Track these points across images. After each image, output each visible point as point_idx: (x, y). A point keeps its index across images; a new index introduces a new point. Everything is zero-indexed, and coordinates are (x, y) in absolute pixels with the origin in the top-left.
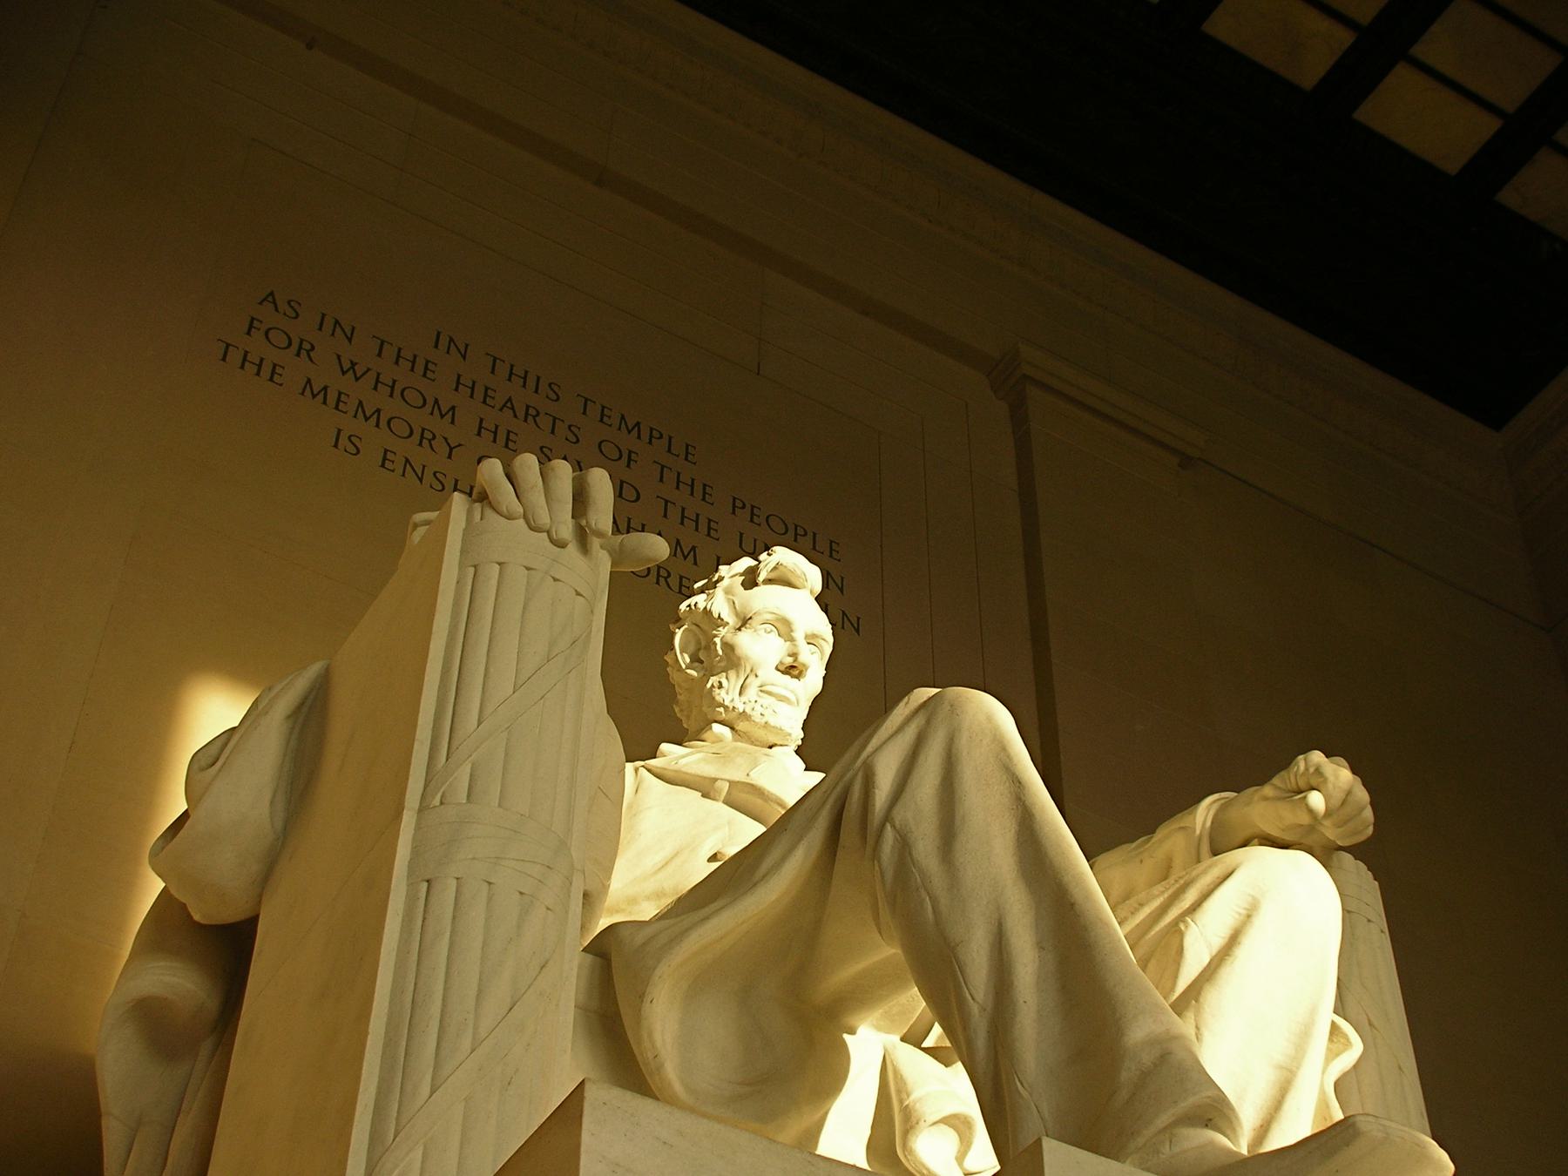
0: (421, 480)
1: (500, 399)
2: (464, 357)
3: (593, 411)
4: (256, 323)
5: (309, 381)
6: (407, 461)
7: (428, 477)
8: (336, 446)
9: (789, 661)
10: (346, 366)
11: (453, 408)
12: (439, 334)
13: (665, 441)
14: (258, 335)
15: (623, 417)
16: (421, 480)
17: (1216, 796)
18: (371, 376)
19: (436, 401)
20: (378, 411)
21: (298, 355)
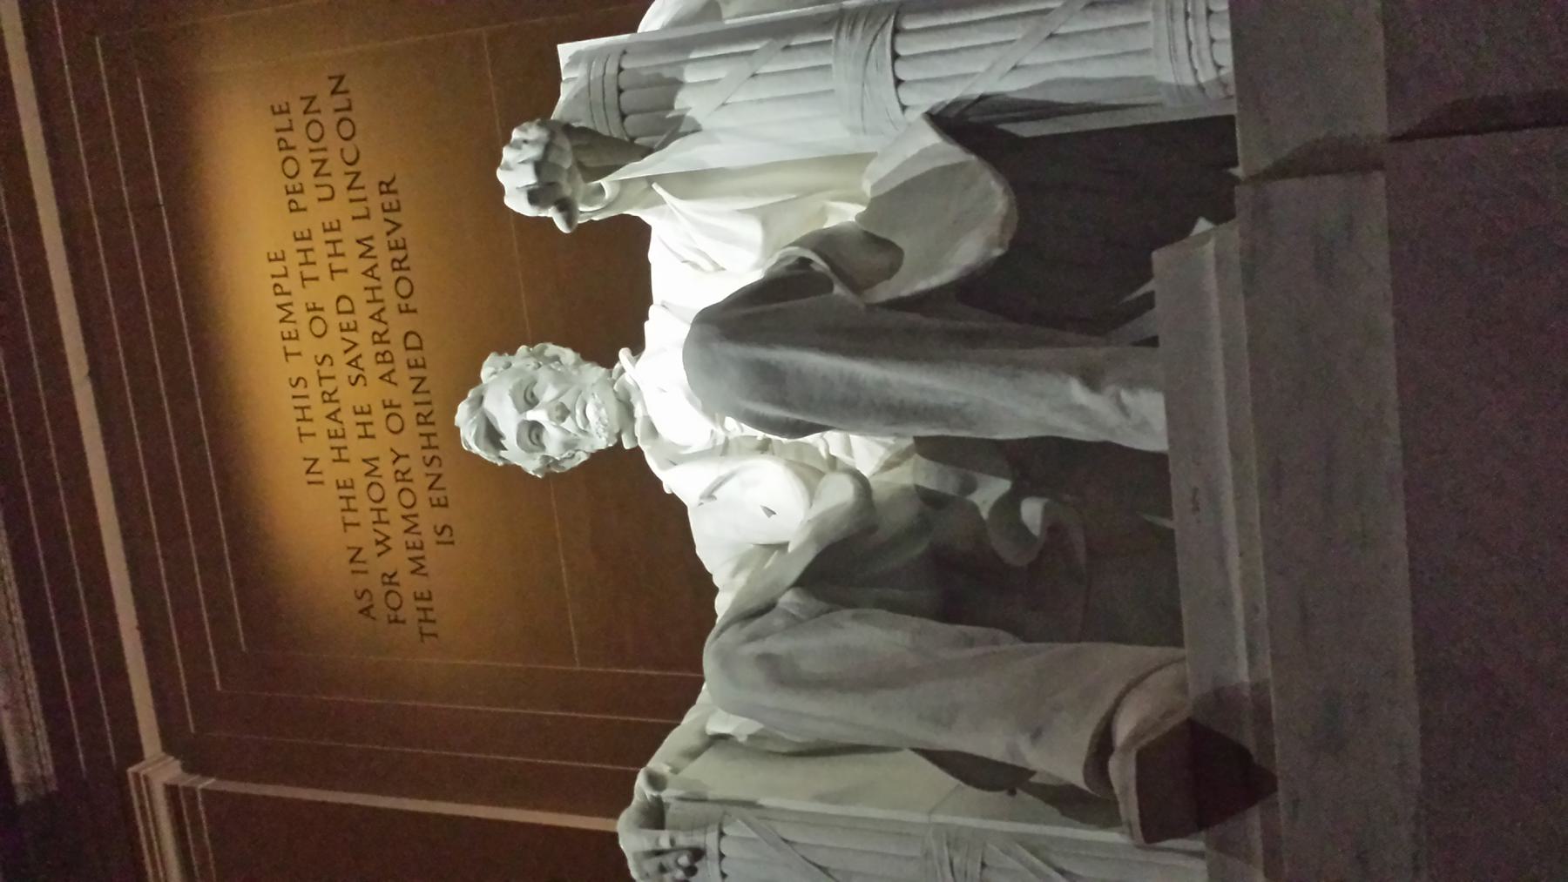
1: (334, 426)
3: (292, 346)
5: (413, 572)
6: (431, 488)
7: (434, 469)
10: (381, 548)
13: (276, 280)
14: (401, 615)
15: (282, 321)
16: (439, 476)
19: (367, 474)
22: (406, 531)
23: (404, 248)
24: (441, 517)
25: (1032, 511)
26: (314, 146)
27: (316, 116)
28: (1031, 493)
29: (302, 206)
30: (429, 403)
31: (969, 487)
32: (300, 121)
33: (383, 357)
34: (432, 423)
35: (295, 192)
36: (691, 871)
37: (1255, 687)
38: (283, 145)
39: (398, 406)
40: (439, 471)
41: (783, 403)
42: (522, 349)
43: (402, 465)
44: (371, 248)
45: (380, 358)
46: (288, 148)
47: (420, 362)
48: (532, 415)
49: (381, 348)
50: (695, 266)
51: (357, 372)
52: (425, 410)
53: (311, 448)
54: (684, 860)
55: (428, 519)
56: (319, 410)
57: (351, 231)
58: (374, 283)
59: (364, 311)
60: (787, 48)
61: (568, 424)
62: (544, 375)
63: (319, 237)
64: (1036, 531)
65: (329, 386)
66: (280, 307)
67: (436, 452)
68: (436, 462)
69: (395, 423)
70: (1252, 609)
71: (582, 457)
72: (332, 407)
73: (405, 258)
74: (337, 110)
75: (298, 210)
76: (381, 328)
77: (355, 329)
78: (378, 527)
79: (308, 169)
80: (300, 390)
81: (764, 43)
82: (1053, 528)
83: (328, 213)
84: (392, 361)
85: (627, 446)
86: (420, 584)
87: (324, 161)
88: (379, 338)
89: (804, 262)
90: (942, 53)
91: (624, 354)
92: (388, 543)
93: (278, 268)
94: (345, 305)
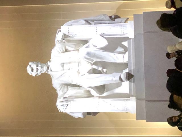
9: (40, 68)
25: (105, 70)
28: (104, 69)
31: (98, 68)
36: (67, 107)
37: (133, 70)
41: (89, 57)
48: (38, 68)
50: (59, 52)
54: (66, 106)
61: (42, 69)
64: (105, 71)
70: (133, 64)
71: (40, 74)
82: (106, 72)
89: (89, 45)
91: (48, 62)
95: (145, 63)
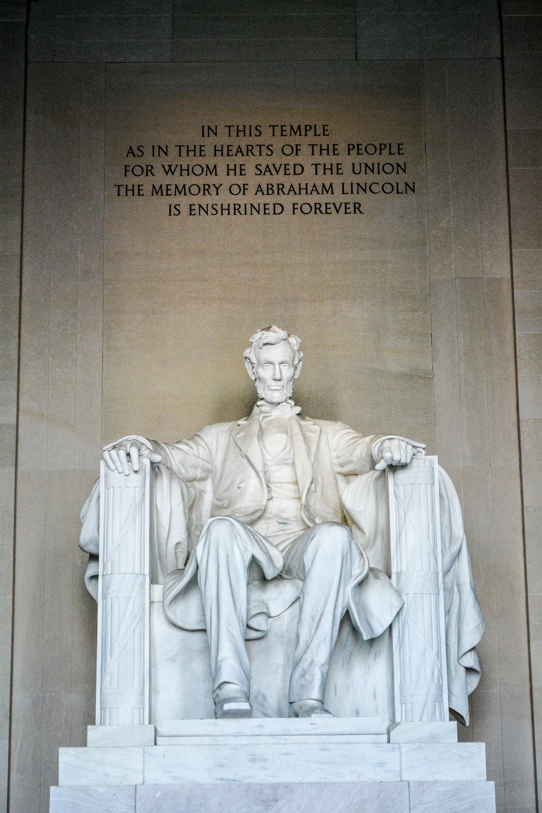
0: (207, 213)
2: (216, 134)
4: (128, 169)
5: (154, 186)
6: (200, 206)
7: (210, 210)
8: (170, 215)
10: (167, 168)
11: (215, 166)
12: (203, 127)
14: (129, 173)
16: (207, 213)
17: (378, 441)
18: (178, 169)
19: (208, 166)
20: (184, 186)
21: (147, 175)
22: (176, 186)
23: (327, 213)
24: (185, 210)
26: (381, 167)
27: (395, 170)
29: (351, 151)
30: (246, 214)
32: (395, 159)
33: (270, 187)
34: (235, 214)
35: (358, 149)
38: (381, 148)
39: (244, 194)
40: (209, 213)
42: (302, 355)
43: (213, 190)
44: (327, 192)
45: (270, 187)
46: (381, 149)
47: (267, 212)
48: (277, 366)
49: (275, 188)
51: (263, 171)
52: (242, 210)
53: (222, 131)
54: (127, 474)
55: (183, 201)
56: (243, 141)
57: (336, 180)
58: (309, 192)
59: (295, 180)
60: (429, 553)
62: (292, 369)
63: (335, 160)
65: (256, 151)
66: (299, 127)
67: (219, 212)
68: (214, 212)
69: (235, 190)
72: (245, 153)
73: (321, 212)
74: (397, 184)
75: (349, 150)
76: (286, 190)
77: (285, 174)
78: (179, 167)
79: (370, 160)
80: (254, 131)
81: (432, 545)
83: (347, 168)
84: (268, 194)
85: (259, 403)
86: (147, 189)
87: (373, 171)
88: (281, 188)
90: (423, 610)
91: (298, 409)
92: (170, 172)
93: (319, 131)
94: (299, 169)
95: (287, 786)
